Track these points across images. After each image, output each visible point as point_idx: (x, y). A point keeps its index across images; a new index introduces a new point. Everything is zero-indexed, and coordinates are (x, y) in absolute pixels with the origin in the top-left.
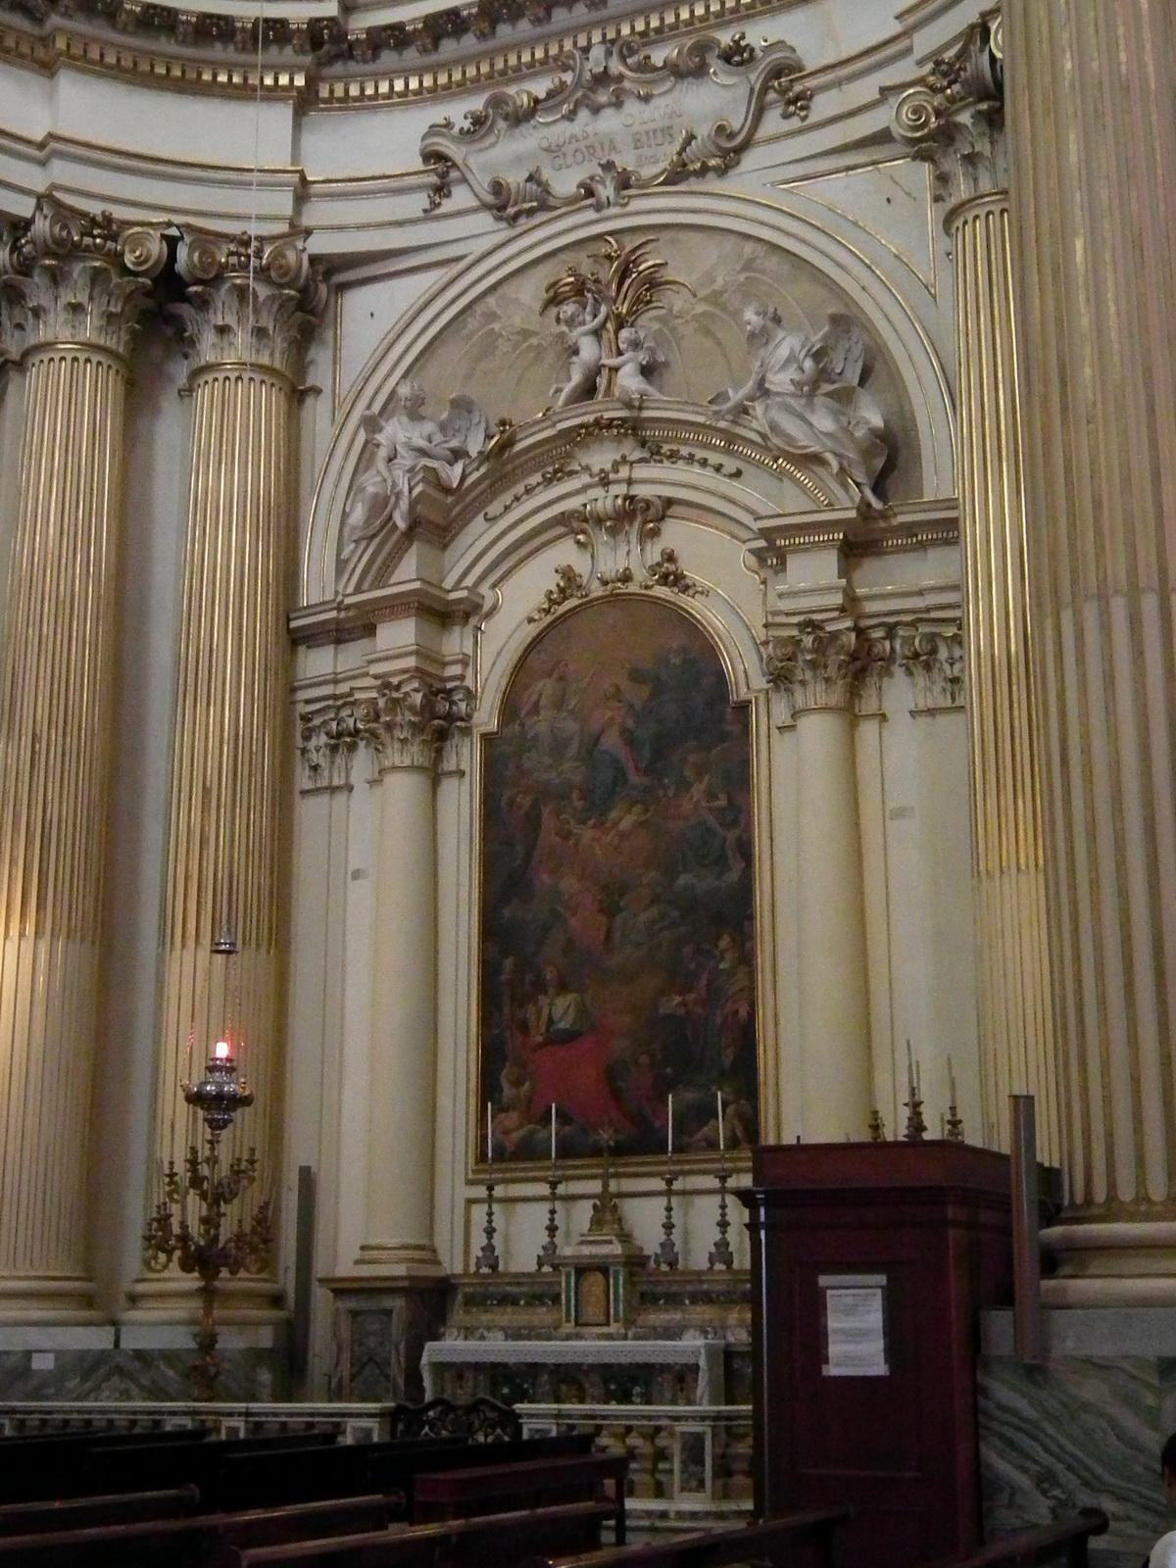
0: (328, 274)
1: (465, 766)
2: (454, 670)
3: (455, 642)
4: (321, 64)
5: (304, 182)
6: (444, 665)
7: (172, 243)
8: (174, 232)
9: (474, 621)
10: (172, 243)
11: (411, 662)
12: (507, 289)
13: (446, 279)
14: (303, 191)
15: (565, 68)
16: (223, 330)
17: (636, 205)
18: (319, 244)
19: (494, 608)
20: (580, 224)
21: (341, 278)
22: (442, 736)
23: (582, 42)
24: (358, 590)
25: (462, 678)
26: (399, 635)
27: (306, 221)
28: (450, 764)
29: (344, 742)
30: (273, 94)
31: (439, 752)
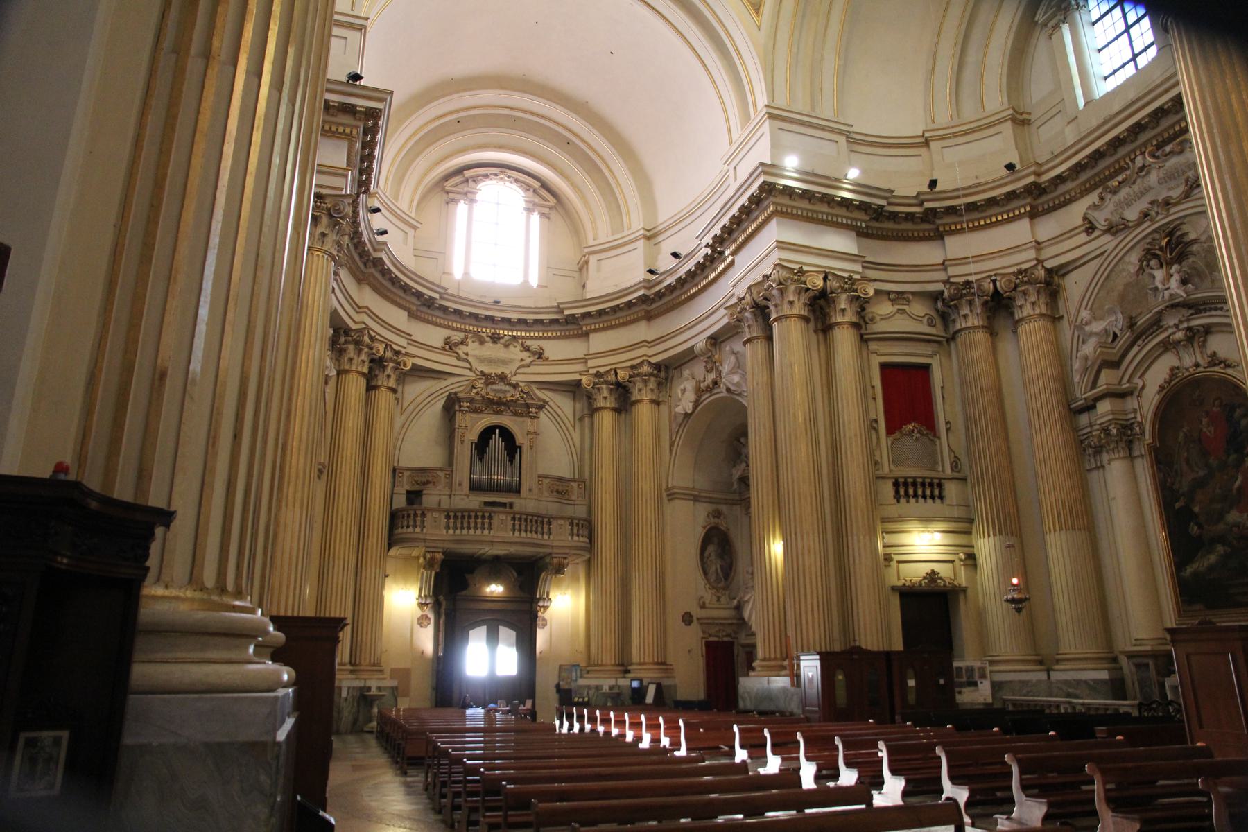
0: (1057, 273)
1: (1143, 453)
2: (1132, 416)
3: (1131, 403)
4: (1035, 199)
5: (1038, 243)
6: (1126, 414)
7: (994, 282)
8: (993, 278)
9: (1136, 393)
10: (994, 282)
11: (1110, 417)
12: (1127, 259)
13: (1101, 261)
14: (1038, 245)
15: (1126, 169)
16: (1021, 307)
17: (1172, 210)
18: (1049, 265)
19: (1143, 387)
20: (1147, 227)
21: (1062, 272)
22: (1130, 442)
23: (1133, 157)
24: (1085, 393)
25: (1135, 418)
26: (1104, 407)
27: (1042, 257)
28: (1136, 453)
29: (1098, 450)
30: (1020, 217)
31: (1130, 450)
